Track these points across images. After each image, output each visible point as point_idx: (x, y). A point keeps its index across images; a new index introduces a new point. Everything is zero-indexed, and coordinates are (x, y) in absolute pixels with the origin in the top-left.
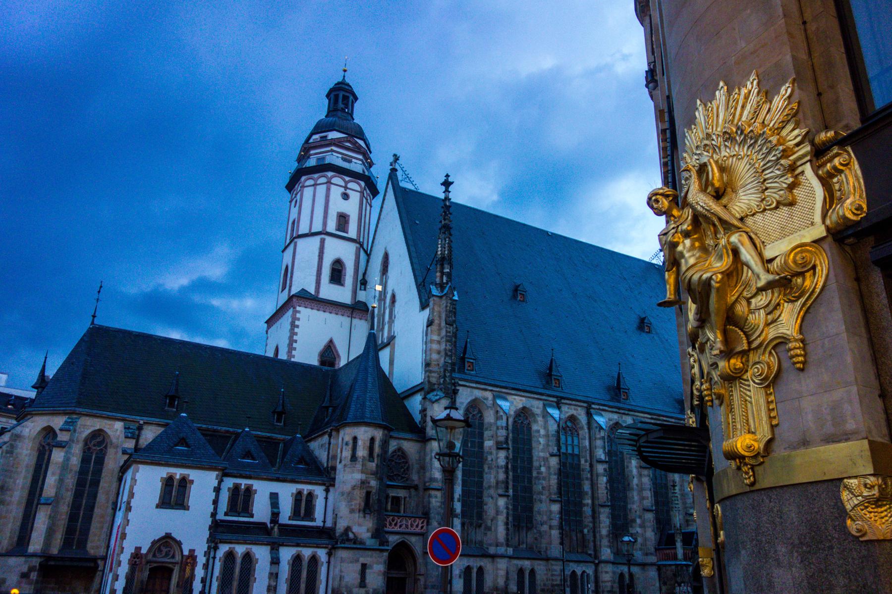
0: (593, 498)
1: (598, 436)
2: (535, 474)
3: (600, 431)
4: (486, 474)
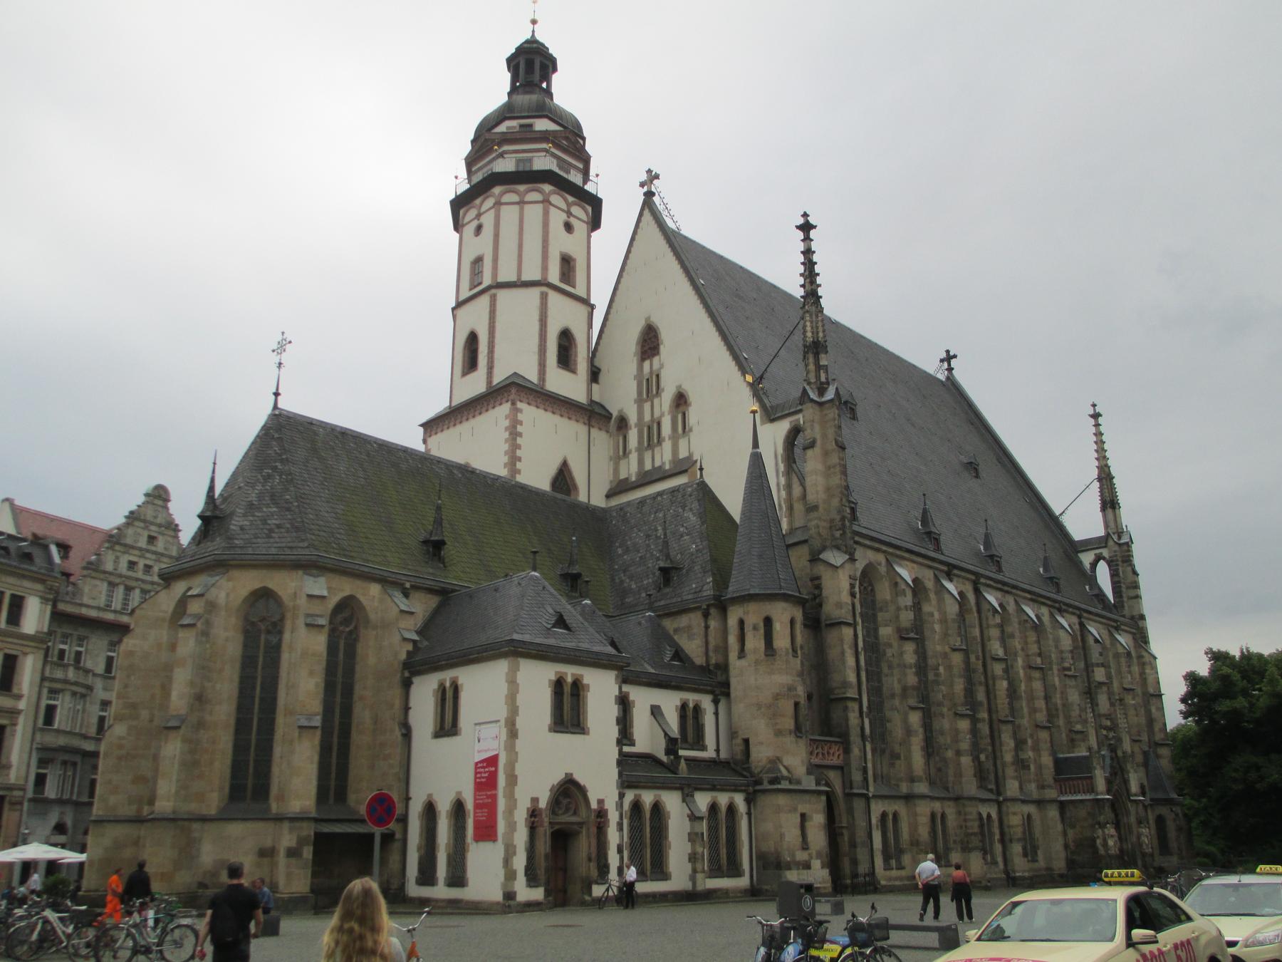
0: (990, 711)
1: (991, 622)
2: (931, 676)
3: (994, 616)
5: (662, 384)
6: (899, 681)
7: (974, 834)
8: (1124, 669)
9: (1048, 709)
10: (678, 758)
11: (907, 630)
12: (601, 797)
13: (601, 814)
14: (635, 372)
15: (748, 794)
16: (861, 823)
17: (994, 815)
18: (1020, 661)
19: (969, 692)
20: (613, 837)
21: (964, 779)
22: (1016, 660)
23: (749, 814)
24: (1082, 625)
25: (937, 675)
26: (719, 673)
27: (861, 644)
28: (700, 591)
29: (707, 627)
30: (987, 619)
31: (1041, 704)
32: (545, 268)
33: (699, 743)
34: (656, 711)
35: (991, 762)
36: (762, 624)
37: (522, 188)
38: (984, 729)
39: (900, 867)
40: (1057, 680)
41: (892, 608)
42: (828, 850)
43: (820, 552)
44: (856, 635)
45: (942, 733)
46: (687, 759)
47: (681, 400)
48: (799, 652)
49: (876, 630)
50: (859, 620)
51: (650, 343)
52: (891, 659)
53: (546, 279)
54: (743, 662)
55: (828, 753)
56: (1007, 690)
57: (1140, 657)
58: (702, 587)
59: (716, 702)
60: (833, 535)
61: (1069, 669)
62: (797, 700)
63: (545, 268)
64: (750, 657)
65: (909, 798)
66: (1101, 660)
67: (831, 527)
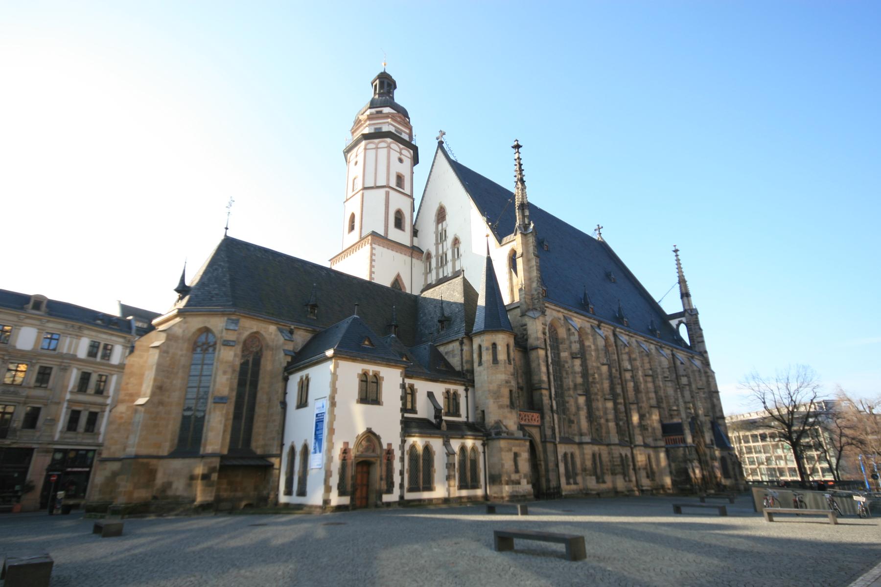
0: (624, 399)
1: (623, 352)
2: (591, 379)
4: (565, 378)
5: (447, 234)
6: (573, 381)
7: (618, 465)
8: (698, 378)
9: (657, 399)
10: (441, 420)
11: (576, 354)
12: (390, 442)
13: (390, 452)
14: (434, 230)
15: (484, 441)
16: (551, 458)
17: (629, 455)
18: (640, 373)
19: (612, 388)
20: (397, 465)
21: (611, 435)
22: (638, 372)
23: (484, 452)
24: (673, 355)
25: (594, 378)
26: (468, 375)
27: (550, 360)
28: (459, 331)
29: (462, 350)
30: (621, 350)
31: (652, 395)
32: (388, 179)
33: (457, 413)
34: (430, 395)
35: (626, 425)
36: (491, 347)
37: (376, 141)
38: (622, 408)
39: (576, 483)
40: (661, 384)
41: (567, 342)
42: (531, 474)
43: (526, 311)
44: (547, 356)
45: (598, 409)
46: (446, 421)
47: (456, 241)
48: (512, 362)
49: (559, 354)
50: (549, 348)
51: (441, 215)
52: (568, 369)
53: (388, 184)
54: (481, 368)
55: (532, 419)
56: (634, 387)
57: (706, 373)
58: (460, 329)
59: (466, 390)
60: (533, 303)
61: (667, 377)
62: (511, 389)
63: (388, 179)
64: (485, 365)
65: (580, 444)
66: (684, 373)
67: (532, 299)
